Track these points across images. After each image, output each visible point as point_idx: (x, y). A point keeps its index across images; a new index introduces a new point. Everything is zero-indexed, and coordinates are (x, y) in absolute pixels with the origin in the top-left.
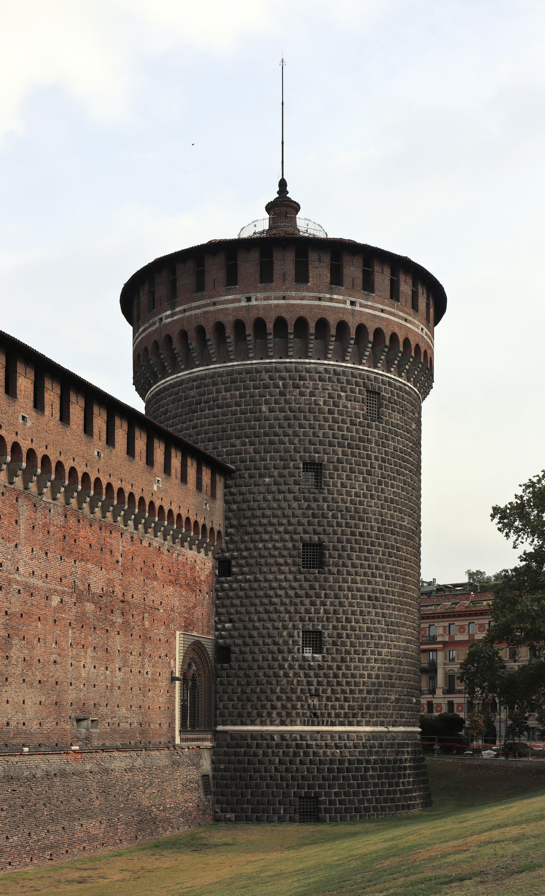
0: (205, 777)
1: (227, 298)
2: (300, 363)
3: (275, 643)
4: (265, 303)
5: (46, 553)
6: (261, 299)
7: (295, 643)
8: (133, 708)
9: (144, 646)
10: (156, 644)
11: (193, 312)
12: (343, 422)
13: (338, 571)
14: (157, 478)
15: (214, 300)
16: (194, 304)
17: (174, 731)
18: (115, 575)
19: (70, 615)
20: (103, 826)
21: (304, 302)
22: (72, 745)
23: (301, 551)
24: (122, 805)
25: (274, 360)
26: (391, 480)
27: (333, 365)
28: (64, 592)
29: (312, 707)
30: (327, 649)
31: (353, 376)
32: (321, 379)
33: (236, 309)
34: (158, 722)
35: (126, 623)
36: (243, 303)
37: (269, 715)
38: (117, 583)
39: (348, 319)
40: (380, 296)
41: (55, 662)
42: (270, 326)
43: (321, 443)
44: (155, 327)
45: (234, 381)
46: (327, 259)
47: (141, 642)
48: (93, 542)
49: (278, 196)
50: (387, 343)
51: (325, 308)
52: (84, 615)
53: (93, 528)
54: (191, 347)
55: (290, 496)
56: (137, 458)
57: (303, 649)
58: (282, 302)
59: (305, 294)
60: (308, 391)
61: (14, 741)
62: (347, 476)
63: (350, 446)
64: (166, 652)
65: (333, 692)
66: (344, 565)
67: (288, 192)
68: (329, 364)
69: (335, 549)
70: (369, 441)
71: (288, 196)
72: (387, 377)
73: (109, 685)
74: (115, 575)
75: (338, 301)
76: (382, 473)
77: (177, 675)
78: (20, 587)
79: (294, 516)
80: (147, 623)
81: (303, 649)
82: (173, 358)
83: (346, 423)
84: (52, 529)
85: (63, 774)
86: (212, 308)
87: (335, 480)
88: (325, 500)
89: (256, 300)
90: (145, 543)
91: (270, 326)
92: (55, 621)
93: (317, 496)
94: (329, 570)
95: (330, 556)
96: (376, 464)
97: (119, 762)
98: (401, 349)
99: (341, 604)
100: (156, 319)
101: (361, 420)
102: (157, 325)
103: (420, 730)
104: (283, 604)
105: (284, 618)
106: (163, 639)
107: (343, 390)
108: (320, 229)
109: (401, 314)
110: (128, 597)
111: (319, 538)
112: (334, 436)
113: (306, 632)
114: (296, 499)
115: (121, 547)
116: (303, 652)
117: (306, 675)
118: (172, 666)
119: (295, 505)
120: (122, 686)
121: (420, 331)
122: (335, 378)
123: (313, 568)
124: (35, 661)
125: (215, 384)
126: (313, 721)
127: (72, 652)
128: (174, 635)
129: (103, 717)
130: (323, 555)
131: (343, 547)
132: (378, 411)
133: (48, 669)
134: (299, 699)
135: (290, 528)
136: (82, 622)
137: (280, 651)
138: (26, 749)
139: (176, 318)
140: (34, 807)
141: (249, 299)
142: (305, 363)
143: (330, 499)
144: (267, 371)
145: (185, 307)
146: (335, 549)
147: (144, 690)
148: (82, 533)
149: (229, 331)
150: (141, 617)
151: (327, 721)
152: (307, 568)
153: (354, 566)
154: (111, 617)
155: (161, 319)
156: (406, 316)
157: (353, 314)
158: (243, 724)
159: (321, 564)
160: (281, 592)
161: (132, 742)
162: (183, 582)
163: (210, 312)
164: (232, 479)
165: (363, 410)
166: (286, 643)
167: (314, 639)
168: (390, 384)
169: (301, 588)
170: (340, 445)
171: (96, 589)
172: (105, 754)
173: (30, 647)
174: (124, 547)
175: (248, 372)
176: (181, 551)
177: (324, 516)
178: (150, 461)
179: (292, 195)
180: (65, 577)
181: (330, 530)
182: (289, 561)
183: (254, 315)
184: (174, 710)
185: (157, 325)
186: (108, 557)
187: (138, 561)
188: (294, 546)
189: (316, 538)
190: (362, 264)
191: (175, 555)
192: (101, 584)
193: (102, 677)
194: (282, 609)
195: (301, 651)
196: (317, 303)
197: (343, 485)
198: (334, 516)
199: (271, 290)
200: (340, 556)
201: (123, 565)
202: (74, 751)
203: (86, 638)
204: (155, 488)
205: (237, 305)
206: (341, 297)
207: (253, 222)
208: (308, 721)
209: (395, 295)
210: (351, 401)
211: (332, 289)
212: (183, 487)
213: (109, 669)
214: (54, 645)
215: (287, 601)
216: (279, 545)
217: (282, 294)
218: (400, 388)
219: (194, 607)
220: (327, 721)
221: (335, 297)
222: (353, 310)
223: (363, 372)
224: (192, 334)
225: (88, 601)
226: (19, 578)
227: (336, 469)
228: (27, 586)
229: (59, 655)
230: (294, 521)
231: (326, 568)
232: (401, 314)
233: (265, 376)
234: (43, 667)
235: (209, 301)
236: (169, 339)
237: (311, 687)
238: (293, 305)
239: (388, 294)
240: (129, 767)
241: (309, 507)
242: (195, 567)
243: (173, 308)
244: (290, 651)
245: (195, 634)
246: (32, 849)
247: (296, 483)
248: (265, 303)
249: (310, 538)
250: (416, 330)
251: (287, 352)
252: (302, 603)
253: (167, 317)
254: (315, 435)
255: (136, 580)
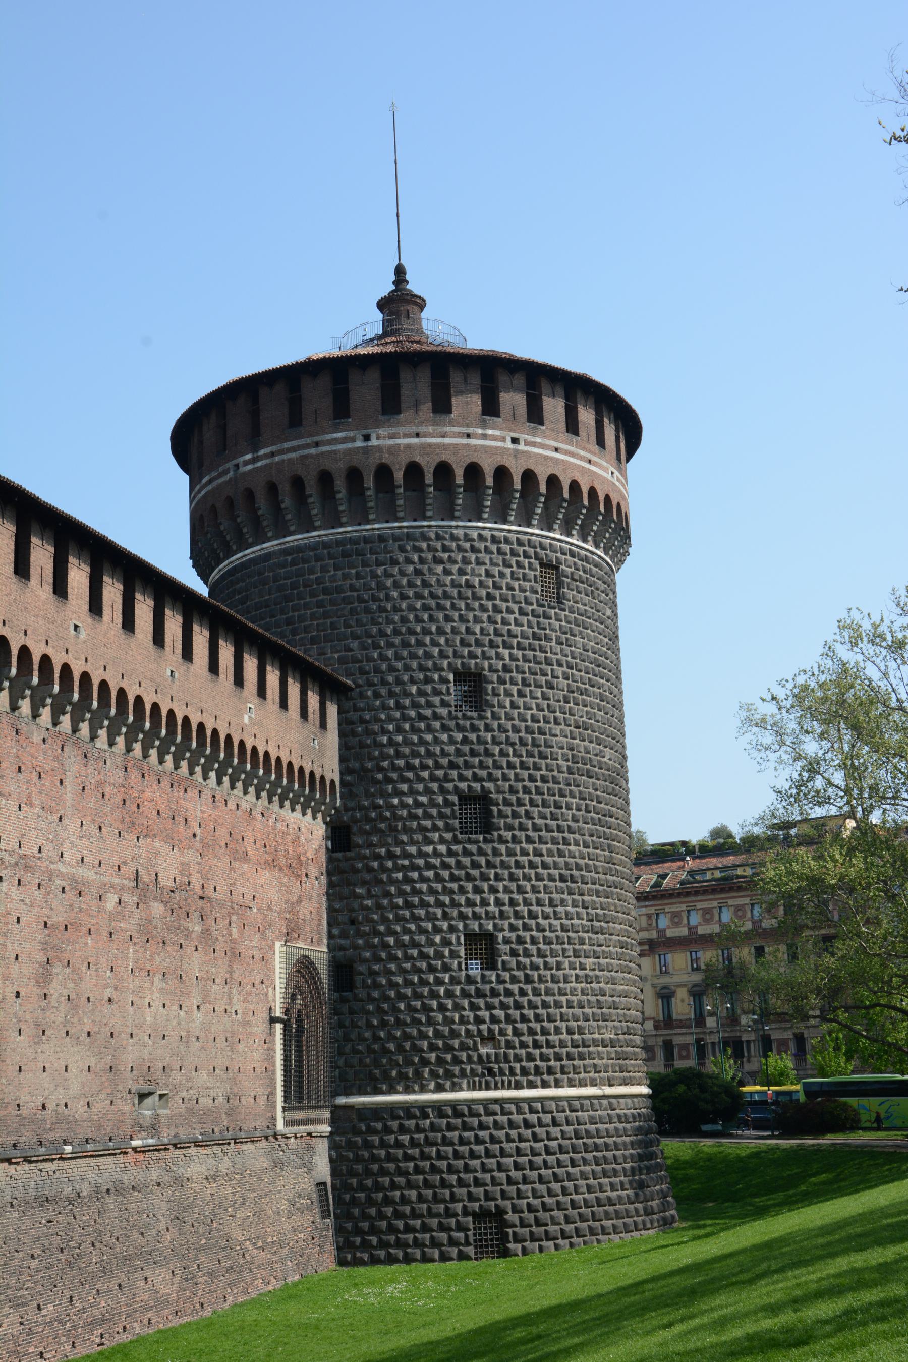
0: (321, 1185)
1: (335, 435)
2: (443, 527)
3: (423, 956)
4: (391, 442)
5: (100, 828)
6: (384, 438)
7: (454, 955)
8: (217, 1071)
9: (231, 967)
10: (248, 964)
11: (285, 457)
12: (509, 611)
13: (514, 836)
14: (249, 705)
15: (316, 439)
16: (286, 445)
17: (275, 1107)
18: (191, 856)
19: (129, 925)
20: (177, 1279)
21: (447, 441)
22: (131, 1138)
23: (456, 808)
24: (203, 1242)
25: (405, 524)
26: (581, 694)
27: (490, 529)
28: (123, 888)
29: (485, 1058)
30: (503, 962)
31: (520, 543)
32: (474, 550)
33: (349, 451)
34: (252, 1094)
35: (206, 932)
36: (359, 444)
37: (418, 1075)
38: (194, 869)
39: (510, 463)
40: (552, 430)
41: (110, 1000)
42: (399, 476)
43: (478, 643)
44: (227, 477)
45: (346, 555)
46: (475, 379)
47: (226, 961)
48: (162, 807)
49: (393, 287)
50: (566, 495)
51: (476, 448)
52: (150, 922)
53: (162, 785)
54: (283, 506)
55: (437, 725)
56: (222, 676)
57: (466, 964)
58: (415, 441)
59: (447, 429)
60: (457, 566)
61: (51, 1136)
62: (519, 691)
63: (520, 647)
64: (262, 976)
65: (516, 1032)
66: (522, 828)
67: (407, 282)
68: (484, 528)
69: (507, 803)
70: (548, 639)
71: (408, 287)
72: (567, 543)
73: (184, 1034)
74: (191, 856)
75: (494, 438)
76: (568, 685)
77: (278, 1013)
78: (64, 884)
79: (443, 753)
80: (235, 931)
81: (466, 964)
82: (256, 522)
83: (513, 613)
84: (107, 790)
85: (117, 1189)
86: (313, 451)
87: (502, 698)
88: (488, 728)
89: (378, 438)
90: (232, 805)
91: (399, 476)
92: (111, 934)
93: (476, 722)
94: (500, 836)
95: (501, 814)
96: (559, 671)
97: (197, 1164)
98: (586, 502)
99: (521, 890)
100: (230, 465)
101: (535, 607)
102: (231, 474)
103: (645, 1090)
104: (432, 891)
105: (435, 914)
106: (258, 957)
107: (506, 564)
108: (456, 333)
109: (582, 453)
110: (209, 891)
111: (483, 787)
112: (497, 633)
113: (470, 935)
114: (445, 728)
115: (199, 813)
116: (466, 969)
117: (474, 1007)
118: (270, 999)
119: (445, 737)
120: (202, 1035)
121: (609, 476)
122: (494, 548)
123: (476, 833)
124: (84, 1000)
125: (318, 559)
126: (487, 1083)
127: (132, 983)
128: (272, 948)
129: (176, 1089)
130: (489, 813)
131: (518, 799)
132: (558, 593)
133: (101, 1011)
134: (464, 1047)
135: (440, 773)
136: (147, 935)
137: (432, 969)
138: (68, 1148)
139: (259, 464)
140: (78, 1251)
141: (367, 438)
142: (451, 527)
143: (495, 727)
144: (396, 538)
145: (273, 448)
146: (507, 803)
147: (233, 1041)
148: (148, 794)
149: (340, 484)
150: (227, 922)
151: (510, 1082)
152: (466, 833)
153: (536, 828)
154: (186, 925)
155: (237, 466)
156: (589, 456)
157: (515, 456)
158: (377, 1091)
159: (487, 827)
160: (430, 874)
161: (216, 1130)
162: (283, 862)
163: (311, 456)
164: (348, 699)
165: (536, 592)
166: (439, 955)
167: (483, 945)
168: (573, 555)
169: (459, 865)
170: (506, 645)
171: (166, 882)
172: (178, 1152)
173: (76, 977)
174: (203, 812)
175: (366, 540)
176: (280, 815)
177: (488, 753)
178: (239, 681)
179: (414, 285)
180: (125, 863)
181: (498, 773)
182: (440, 824)
183: (373, 461)
184: (274, 1073)
185: (231, 474)
186: (181, 828)
187: (222, 832)
188: (446, 801)
189: (477, 786)
190: (524, 386)
191: (271, 821)
192: (173, 872)
193: (174, 1023)
194: (431, 900)
195: (463, 967)
196: (465, 441)
197: (514, 706)
198: (503, 753)
199: (399, 424)
200: (515, 815)
201: (202, 841)
202: (135, 1149)
203: (152, 959)
204: (246, 720)
205: (350, 445)
206: (498, 433)
207: (363, 325)
208: (480, 1082)
209: (572, 427)
210: (518, 579)
211: (484, 421)
212: (283, 714)
213: (184, 1008)
214: (109, 973)
215: (438, 887)
216: (424, 799)
217: (414, 429)
218: (586, 559)
219: (299, 901)
220: (510, 1082)
221: (490, 432)
222: (517, 451)
223: (534, 538)
224: (285, 489)
225: (155, 899)
226: (63, 870)
227: (502, 681)
228: (74, 880)
229: (116, 989)
230: (444, 761)
231: (495, 834)
232: (582, 453)
233: (393, 545)
234: (93, 1010)
235: (308, 441)
236: (250, 495)
237: (481, 1027)
238: (430, 445)
239: (562, 426)
240: (212, 1173)
241: (465, 740)
242: (298, 838)
243: (255, 449)
244: (446, 968)
245: (300, 945)
246: (75, 1327)
247: (444, 704)
248: (391, 442)
249: (469, 787)
250: (605, 474)
251: (424, 511)
252: (462, 890)
253: (246, 463)
254: (468, 631)
255: (220, 863)
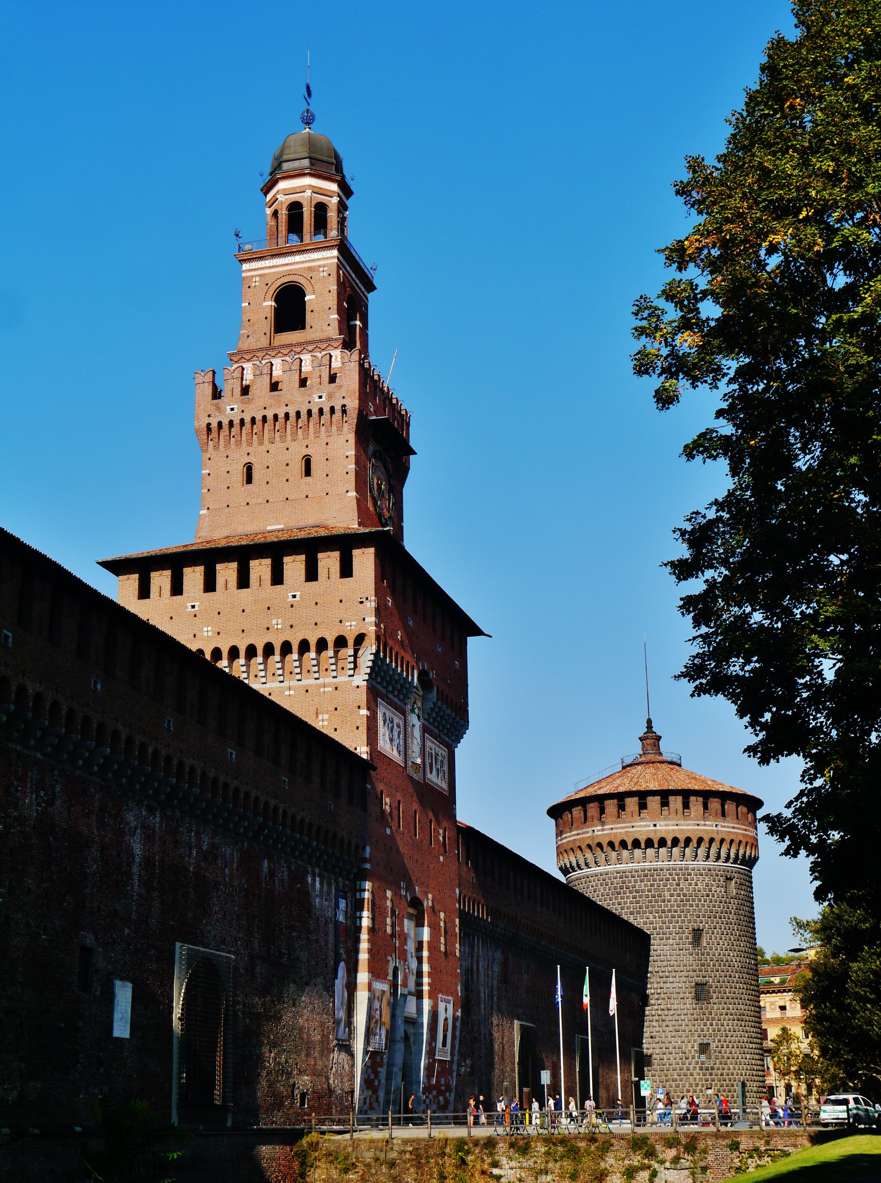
21: (689, 827)
58: (676, 827)
75: (709, 826)
183: (659, 836)
196: (697, 827)
206: (710, 823)
217: (676, 822)
